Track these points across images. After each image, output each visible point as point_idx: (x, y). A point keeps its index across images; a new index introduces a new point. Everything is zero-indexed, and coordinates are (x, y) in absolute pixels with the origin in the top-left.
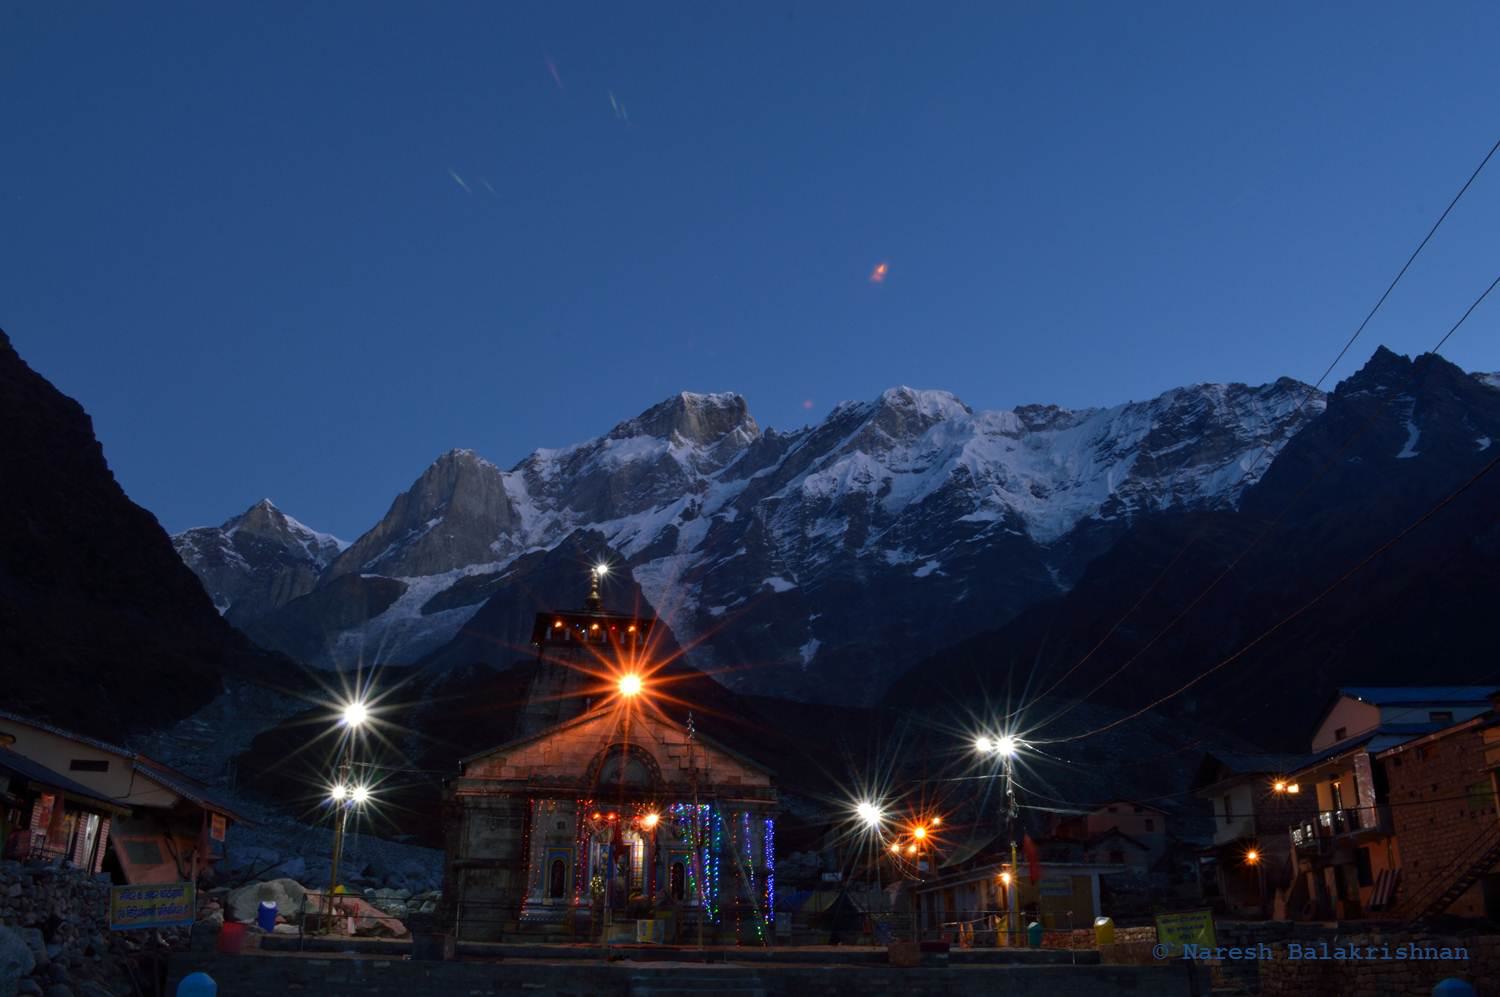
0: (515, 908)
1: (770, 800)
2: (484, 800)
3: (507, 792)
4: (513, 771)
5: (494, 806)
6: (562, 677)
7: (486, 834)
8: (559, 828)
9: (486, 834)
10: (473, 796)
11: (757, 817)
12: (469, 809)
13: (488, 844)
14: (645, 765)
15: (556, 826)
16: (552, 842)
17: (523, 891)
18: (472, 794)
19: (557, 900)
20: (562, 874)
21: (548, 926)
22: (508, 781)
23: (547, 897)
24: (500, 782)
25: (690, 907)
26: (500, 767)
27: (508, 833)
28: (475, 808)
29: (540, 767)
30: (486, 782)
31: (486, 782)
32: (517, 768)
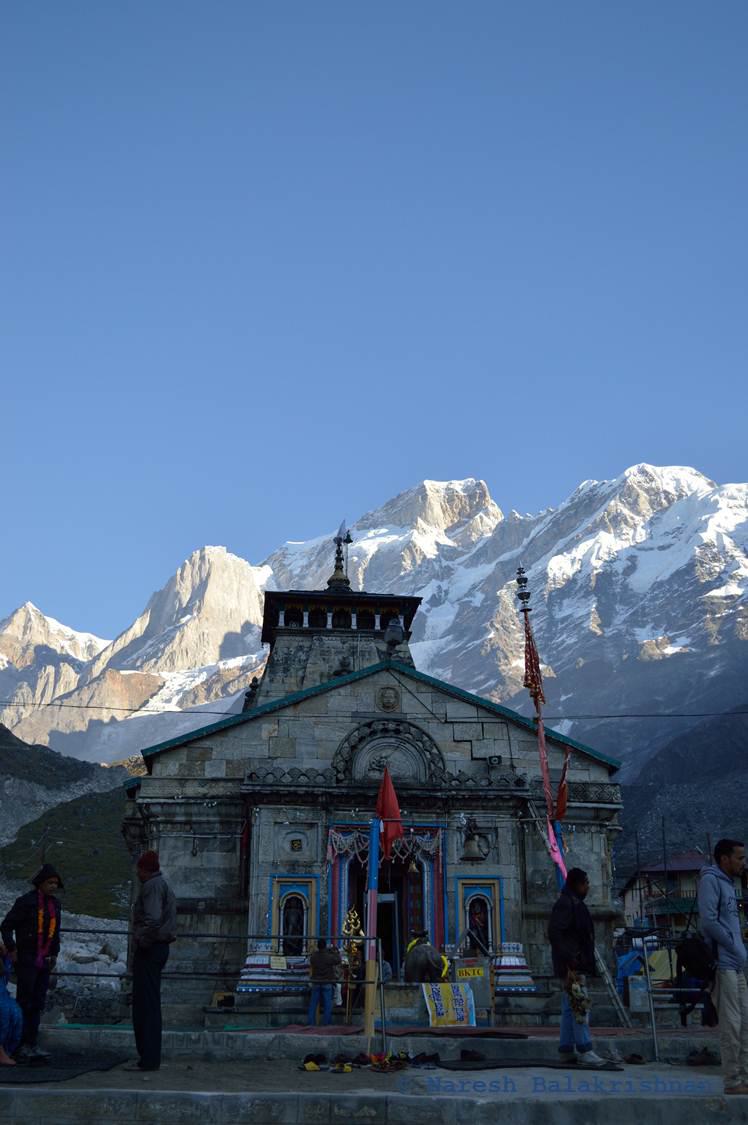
0: (229, 975)
1: (612, 803)
2: (178, 809)
3: (213, 797)
4: (224, 767)
5: (194, 819)
6: (300, 673)
7: (185, 861)
8: (293, 849)
9: (185, 861)
10: (162, 804)
11: (593, 829)
12: (158, 824)
13: (187, 875)
14: (421, 752)
15: (287, 846)
16: (282, 870)
17: (239, 945)
18: (162, 801)
19: (294, 960)
20: (300, 920)
21: (280, 1000)
22: (215, 780)
23: (277, 954)
24: (205, 782)
25: (500, 967)
26: (204, 761)
27: (217, 859)
28: (166, 822)
29: (262, 760)
30: (182, 781)
31: (182, 781)
32: (228, 762)
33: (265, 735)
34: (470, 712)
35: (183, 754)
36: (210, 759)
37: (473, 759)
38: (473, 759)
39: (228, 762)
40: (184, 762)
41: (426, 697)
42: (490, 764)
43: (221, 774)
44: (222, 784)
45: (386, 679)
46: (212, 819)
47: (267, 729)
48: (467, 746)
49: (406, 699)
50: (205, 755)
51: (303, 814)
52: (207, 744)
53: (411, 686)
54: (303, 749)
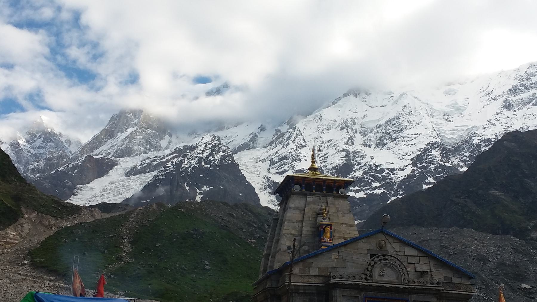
5: (307, 292)
26: (309, 268)
28: (296, 293)
32: (319, 268)
33: (333, 257)
34: (413, 252)
35: (301, 265)
36: (312, 267)
37: (416, 271)
38: (416, 271)
39: (319, 268)
40: (302, 268)
41: (396, 246)
42: (422, 274)
43: (316, 273)
44: (318, 278)
45: (381, 236)
46: (313, 292)
47: (334, 255)
48: (413, 265)
49: (388, 245)
50: (310, 266)
51: (354, 293)
52: (311, 260)
53: (390, 240)
54: (349, 264)
